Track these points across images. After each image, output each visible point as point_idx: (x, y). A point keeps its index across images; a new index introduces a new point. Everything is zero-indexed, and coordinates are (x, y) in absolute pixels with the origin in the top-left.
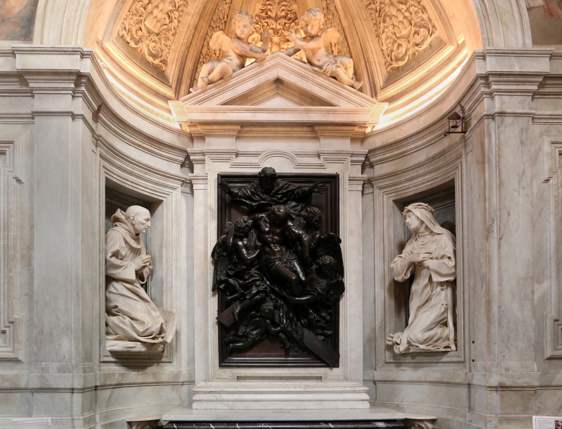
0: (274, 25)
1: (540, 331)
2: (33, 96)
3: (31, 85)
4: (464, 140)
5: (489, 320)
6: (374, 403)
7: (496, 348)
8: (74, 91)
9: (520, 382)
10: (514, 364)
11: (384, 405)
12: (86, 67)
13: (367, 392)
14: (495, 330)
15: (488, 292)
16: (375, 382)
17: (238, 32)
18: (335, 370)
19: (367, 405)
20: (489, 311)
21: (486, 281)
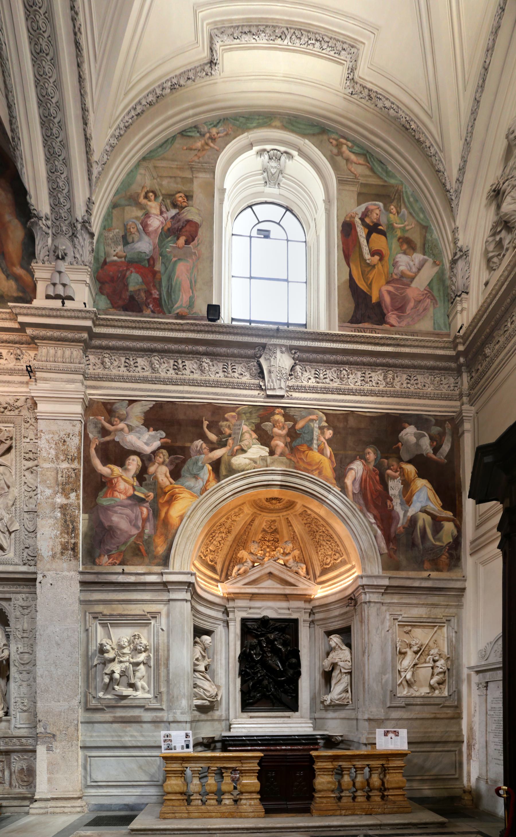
0: (267, 544)
1: (385, 696)
2: (169, 592)
3: (169, 587)
4: (355, 610)
5: (364, 691)
6: (314, 729)
7: (367, 703)
8: (187, 590)
9: (376, 717)
10: (374, 710)
11: (319, 730)
12: (192, 579)
13: (312, 723)
14: (367, 695)
15: (364, 678)
16: (315, 719)
17: (252, 551)
18: (296, 713)
19: (312, 729)
20: (364, 687)
21: (363, 673)
